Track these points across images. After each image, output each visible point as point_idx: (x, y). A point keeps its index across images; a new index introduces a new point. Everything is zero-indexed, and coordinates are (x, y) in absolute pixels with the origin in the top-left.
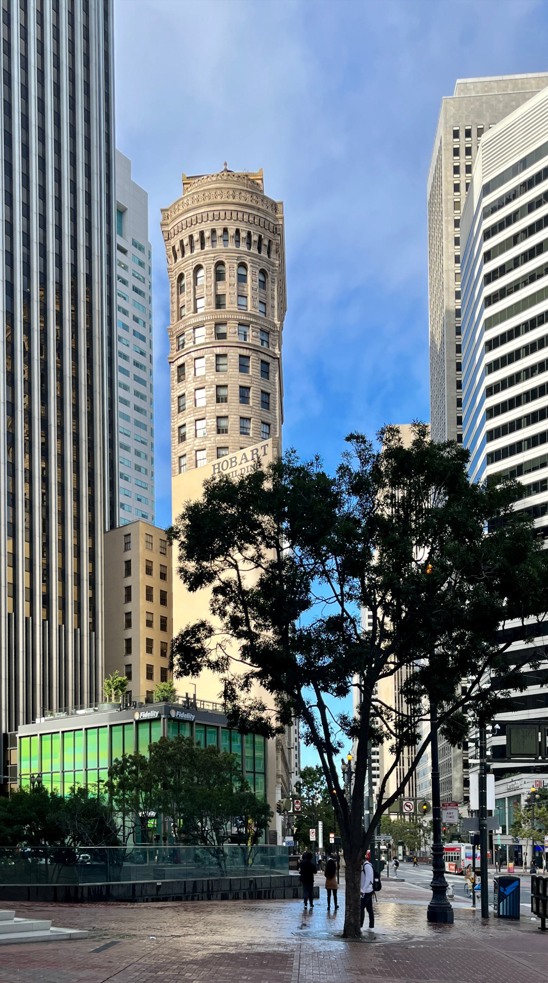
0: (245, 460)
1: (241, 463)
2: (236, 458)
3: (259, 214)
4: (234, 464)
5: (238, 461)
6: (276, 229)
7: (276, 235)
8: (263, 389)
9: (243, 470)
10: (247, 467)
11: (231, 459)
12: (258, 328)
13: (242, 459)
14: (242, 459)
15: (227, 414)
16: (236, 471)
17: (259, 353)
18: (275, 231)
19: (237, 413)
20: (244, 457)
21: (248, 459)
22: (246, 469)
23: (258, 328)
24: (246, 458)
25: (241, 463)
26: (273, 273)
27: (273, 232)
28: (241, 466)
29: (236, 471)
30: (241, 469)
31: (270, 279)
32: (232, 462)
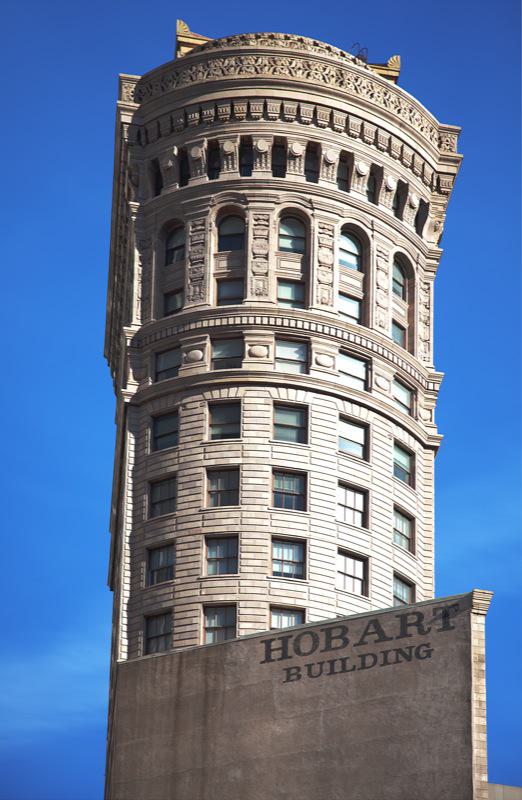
5: (353, 639)
10: (385, 653)
14: (366, 633)
24: (380, 631)
25: (362, 643)
28: (364, 650)
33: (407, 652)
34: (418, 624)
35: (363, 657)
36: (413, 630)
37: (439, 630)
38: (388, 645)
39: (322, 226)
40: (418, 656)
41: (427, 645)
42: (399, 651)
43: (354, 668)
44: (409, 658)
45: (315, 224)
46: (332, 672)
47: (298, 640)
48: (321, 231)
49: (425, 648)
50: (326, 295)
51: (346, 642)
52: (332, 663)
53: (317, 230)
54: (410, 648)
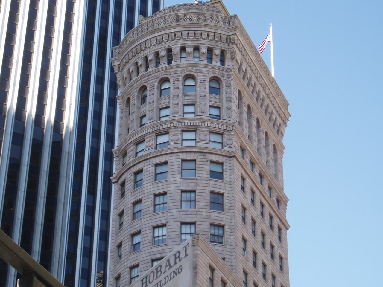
0: (168, 267)
1: (165, 271)
3: (207, 30)
4: (159, 273)
5: (163, 270)
6: (230, 39)
7: (230, 44)
8: (213, 189)
9: (167, 278)
10: (171, 274)
11: (157, 269)
12: (207, 131)
13: (166, 266)
14: (166, 266)
15: (164, 222)
16: (160, 282)
17: (207, 155)
18: (228, 41)
19: (178, 219)
21: (171, 266)
22: (169, 276)
23: (207, 131)
24: (170, 265)
25: (165, 271)
26: (229, 78)
27: (227, 42)
29: (160, 282)
30: (165, 278)
31: (224, 84)
32: (157, 272)
33: (176, 271)
34: (179, 257)
35: (165, 278)
36: (178, 260)
37: (184, 257)
40: (179, 273)
41: (181, 266)
42: (174, 272)
44: (176, 274)
45: (198, 78)
47: (149, 277)
49: (180, 268)
50: (203, 108)
52: (157, 284)
53: (199, 81)
54: (177, 269)
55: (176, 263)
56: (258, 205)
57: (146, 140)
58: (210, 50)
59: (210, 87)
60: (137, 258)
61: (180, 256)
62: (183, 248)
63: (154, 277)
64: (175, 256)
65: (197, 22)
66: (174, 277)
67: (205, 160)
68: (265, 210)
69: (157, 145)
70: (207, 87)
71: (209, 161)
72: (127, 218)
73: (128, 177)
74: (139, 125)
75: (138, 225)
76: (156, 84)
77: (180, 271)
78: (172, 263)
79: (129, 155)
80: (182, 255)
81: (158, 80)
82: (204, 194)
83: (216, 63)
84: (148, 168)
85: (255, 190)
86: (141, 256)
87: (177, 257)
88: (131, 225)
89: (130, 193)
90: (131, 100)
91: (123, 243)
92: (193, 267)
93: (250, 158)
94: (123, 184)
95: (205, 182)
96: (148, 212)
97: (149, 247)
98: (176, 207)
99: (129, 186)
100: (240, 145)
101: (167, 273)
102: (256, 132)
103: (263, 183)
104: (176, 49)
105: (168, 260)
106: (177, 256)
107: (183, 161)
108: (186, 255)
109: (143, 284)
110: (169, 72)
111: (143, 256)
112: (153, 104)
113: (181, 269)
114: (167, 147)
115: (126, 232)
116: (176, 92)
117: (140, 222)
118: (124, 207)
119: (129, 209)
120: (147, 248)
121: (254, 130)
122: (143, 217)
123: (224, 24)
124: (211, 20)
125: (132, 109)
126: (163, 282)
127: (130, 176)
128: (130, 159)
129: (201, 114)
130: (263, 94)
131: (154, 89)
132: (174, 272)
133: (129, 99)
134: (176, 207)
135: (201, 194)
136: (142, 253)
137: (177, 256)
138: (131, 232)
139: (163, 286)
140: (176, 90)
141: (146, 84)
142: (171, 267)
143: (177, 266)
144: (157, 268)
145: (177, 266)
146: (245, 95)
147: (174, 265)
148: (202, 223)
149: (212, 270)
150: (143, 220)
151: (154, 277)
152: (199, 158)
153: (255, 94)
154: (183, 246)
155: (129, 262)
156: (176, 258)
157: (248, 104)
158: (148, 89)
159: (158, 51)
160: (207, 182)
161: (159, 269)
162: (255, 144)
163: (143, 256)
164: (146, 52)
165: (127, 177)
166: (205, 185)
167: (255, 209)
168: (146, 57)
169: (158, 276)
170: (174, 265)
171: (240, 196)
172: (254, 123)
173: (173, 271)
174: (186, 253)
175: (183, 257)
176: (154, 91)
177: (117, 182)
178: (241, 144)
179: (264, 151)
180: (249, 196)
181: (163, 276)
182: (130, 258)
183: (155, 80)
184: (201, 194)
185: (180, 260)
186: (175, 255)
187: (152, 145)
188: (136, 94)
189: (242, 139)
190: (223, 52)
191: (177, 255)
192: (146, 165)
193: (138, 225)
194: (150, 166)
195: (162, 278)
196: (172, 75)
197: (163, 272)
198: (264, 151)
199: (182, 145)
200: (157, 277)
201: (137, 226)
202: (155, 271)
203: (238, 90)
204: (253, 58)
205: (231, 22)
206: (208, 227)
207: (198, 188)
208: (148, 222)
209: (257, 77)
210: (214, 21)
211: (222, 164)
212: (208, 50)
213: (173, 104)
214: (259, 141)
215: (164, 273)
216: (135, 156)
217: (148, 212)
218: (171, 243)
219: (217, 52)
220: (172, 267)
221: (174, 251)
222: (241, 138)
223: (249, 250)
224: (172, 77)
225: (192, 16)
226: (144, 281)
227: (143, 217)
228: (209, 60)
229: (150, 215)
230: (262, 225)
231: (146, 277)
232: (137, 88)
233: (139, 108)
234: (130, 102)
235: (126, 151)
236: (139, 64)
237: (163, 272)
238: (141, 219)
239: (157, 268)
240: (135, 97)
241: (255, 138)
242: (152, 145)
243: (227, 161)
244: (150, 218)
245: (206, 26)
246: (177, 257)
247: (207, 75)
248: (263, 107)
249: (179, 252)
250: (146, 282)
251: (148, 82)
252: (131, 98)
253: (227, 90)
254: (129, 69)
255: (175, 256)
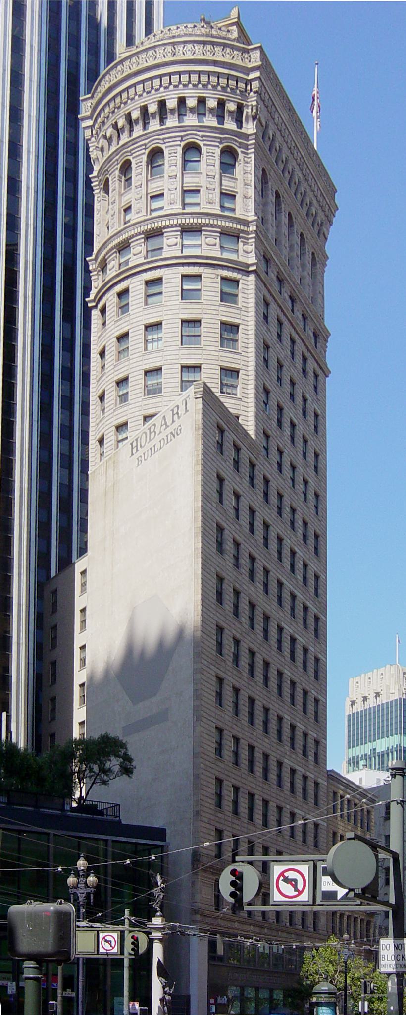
0: (164, 427)
2: (155, 425)
4: (153, 434)
8: (224, 319)
10: (167, 436)
13: (162, 426)
19: (177, 361)
20: (163, 423)
24: (166, 423)
25: (160, 432)
29: (154, 446)
31: (241, 156)
32: (150, 433)
34: (177, 413)
35: (160, 441)
37: (184, 414)
38: (169, 430)
39: (208, 151)
40: (178, 435)
41: (180, 426)
42: (171, 433)
43: (158, 451)
44: (174, 436)
45: (204, 149)
46: (151, 455)
47: (141, 439)
48: (208, 154)
49: (179, 428)
51: (155, 433)
52: (151, 449)
54: (175, 430)
55: (173, 421)
56: (287, 342)
57: (132, 245)
58: (221, 104)
59: (221, 163)
60: (125, 414)
61: (179, 412)
62: (183, 401)
63: (146, 440)
64: (173, 413)
65: (202, 57)
66: (171, 440)
67: (213, 276)
68: (296, 348)
69: (147, 252)
70: (218, 163)
71: (220, 278)
72: (110, 356)
73: (109, 299)
74: (122, 222)
75: (126, 368)
76: (145, 157)
77: (179, 432)
78: (169, 422)
79: (109, 266)
80: (182, 411)
81: (147, 151)
82: (212, 326)
83: (230, 125)
84: (136, 285)
85: (284, 320)
86: (130, 411)
87: (175, 414)
88: (116, 369)
89: (113, 322)
90: (110, 183)
91: (106, 393)
92: (195, 427)
93: (278, 272)
94: (103, 311)
95: (213, 307)
96: (137, 351)
97: (140, 399)
98: (174, 343)
99: (111, 311)
100: (262, 254)
101: (163, 435)
102: (287, 234)
103: (295, 309)
104: (172, 104)
105: (164, 417)
106: (175, 412)
107: (184, 277)
108: (187, 411)
109: (132, 448)
110: (164, 139)
111: (133, 410)
112: (140, 189)
113: (180, 430)
114: (161, 255)
115: (109, 377)
116: (173, 171)
117: (127, 363)
118: (105, 342)
119: (112, 345)
120: (137, 400)
121: (285, 230)
122: (131, 357)
123: (242, 60)
124: (223, 52)
125: (112, 197)
126: (158, 446)
127: (112, 297)
128: (111, 273)
129: (209, 206)
130: (298, 175)
131: (141, 165)
132: (171, 433)
133: (107, 180)
134: (174, 343)
135: (209, 325)
136: (130, 407)
137: (175, 412)
138: (116, 378)
139: (158, 451)
140: (173, 168)
141: (130, 158)
142: (167, 426)
143: (175, 425)
144: (150, 428)
145: (175, 425)
146: (271, 174)
147: (171, 424)
148: (208, 366)
149: (222, 431)
150: (131, 362)
151: (146, 440)
152: (205, 272)
153: (286, 174)
154: (183, 398)
155: (115, 418)
156: (173, 415)
157: (277, 191)
158: (133, 165)
159: (146, 105)
160: (217, 308)
161: (152, 430)
162: (285, 252)
163: (133, 410)
164: (130, 106)
165: (108, 300)
166: (214, 312)
167: (281, 347)
168: (129, 114)
169: (151, 438)
170: (171, 424)
171: (262, 328)
172: (285, 220)
173: (170, 431)
174: (186, 408)
175: (183, 413)
176: (142, 168)
177: (96, 307)
178: (264, 252)
179: (297, 262)
180: (274, 328)
181: (158, 438)
182: (115, 413)
183: (143, 151)
184: (209, 325)
185: (179, 418)
186: (173, 410)
187: (141, 252)
188: (117, 173)
189: (267, 245)
190: (240, 108)
191: (175, 412)
192: (133, 281)
193: (126, 368)
194: (139, 283)
195: (155, 441)
196: (167, 144)
197: (158, 432)
198: (297, 262)
199: (182, 252)
200: (150, 440)
201: (123, 370)
202: (148, 432)
203: (261, 169)
204: (285, 116)
205: (252, 56)
206: (218, 372)
207: (205, 316)
208: (138, 364)
209: (290, 149)
210: (228, 56)
211: (237, 282)
212: (218, 104)
213: (169, 190)
214: (291, 247)
215: (158, 435)
216: (117, 269)
217: (137, 351)
218: (168, 394)
219: (231, 106)
220: (169, 426)
221: (172, 405)
222: (265, 243)
223: (273, 404)
224: (167, 147)
225: (194, 47)
226: (134, 444)
227: (131, 357)
228: (221, 119)
229: (140, 354)
230: (292, 370)
231: (137, 440)
232: (117, 164)
233: (121, 195)
234: (109, 186)
235: (106, 260)
236: (120, 125)
237: (157, 433)
238: (129, 360)
239: (150, 428)
240: (115, 178)
241: (285, 242)
242: (141, 252)
243: (244, 277)
244: (141, 358)
245: (215, 63)
246: (175, 414)
247: (218, 144)
248: (299, 196)
249: (178, 407)
250: (137, 446)
251: (134, 155)
252: (110, 179)
253: (245, 168)
254: (106, 133)
255: (173, 413)
